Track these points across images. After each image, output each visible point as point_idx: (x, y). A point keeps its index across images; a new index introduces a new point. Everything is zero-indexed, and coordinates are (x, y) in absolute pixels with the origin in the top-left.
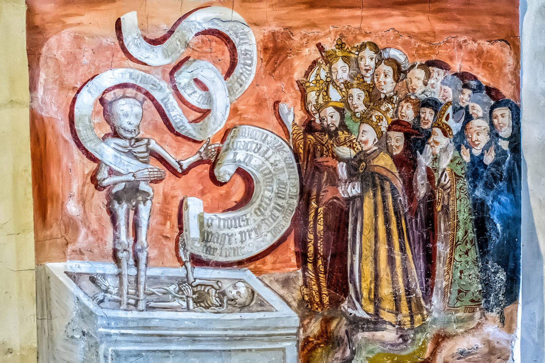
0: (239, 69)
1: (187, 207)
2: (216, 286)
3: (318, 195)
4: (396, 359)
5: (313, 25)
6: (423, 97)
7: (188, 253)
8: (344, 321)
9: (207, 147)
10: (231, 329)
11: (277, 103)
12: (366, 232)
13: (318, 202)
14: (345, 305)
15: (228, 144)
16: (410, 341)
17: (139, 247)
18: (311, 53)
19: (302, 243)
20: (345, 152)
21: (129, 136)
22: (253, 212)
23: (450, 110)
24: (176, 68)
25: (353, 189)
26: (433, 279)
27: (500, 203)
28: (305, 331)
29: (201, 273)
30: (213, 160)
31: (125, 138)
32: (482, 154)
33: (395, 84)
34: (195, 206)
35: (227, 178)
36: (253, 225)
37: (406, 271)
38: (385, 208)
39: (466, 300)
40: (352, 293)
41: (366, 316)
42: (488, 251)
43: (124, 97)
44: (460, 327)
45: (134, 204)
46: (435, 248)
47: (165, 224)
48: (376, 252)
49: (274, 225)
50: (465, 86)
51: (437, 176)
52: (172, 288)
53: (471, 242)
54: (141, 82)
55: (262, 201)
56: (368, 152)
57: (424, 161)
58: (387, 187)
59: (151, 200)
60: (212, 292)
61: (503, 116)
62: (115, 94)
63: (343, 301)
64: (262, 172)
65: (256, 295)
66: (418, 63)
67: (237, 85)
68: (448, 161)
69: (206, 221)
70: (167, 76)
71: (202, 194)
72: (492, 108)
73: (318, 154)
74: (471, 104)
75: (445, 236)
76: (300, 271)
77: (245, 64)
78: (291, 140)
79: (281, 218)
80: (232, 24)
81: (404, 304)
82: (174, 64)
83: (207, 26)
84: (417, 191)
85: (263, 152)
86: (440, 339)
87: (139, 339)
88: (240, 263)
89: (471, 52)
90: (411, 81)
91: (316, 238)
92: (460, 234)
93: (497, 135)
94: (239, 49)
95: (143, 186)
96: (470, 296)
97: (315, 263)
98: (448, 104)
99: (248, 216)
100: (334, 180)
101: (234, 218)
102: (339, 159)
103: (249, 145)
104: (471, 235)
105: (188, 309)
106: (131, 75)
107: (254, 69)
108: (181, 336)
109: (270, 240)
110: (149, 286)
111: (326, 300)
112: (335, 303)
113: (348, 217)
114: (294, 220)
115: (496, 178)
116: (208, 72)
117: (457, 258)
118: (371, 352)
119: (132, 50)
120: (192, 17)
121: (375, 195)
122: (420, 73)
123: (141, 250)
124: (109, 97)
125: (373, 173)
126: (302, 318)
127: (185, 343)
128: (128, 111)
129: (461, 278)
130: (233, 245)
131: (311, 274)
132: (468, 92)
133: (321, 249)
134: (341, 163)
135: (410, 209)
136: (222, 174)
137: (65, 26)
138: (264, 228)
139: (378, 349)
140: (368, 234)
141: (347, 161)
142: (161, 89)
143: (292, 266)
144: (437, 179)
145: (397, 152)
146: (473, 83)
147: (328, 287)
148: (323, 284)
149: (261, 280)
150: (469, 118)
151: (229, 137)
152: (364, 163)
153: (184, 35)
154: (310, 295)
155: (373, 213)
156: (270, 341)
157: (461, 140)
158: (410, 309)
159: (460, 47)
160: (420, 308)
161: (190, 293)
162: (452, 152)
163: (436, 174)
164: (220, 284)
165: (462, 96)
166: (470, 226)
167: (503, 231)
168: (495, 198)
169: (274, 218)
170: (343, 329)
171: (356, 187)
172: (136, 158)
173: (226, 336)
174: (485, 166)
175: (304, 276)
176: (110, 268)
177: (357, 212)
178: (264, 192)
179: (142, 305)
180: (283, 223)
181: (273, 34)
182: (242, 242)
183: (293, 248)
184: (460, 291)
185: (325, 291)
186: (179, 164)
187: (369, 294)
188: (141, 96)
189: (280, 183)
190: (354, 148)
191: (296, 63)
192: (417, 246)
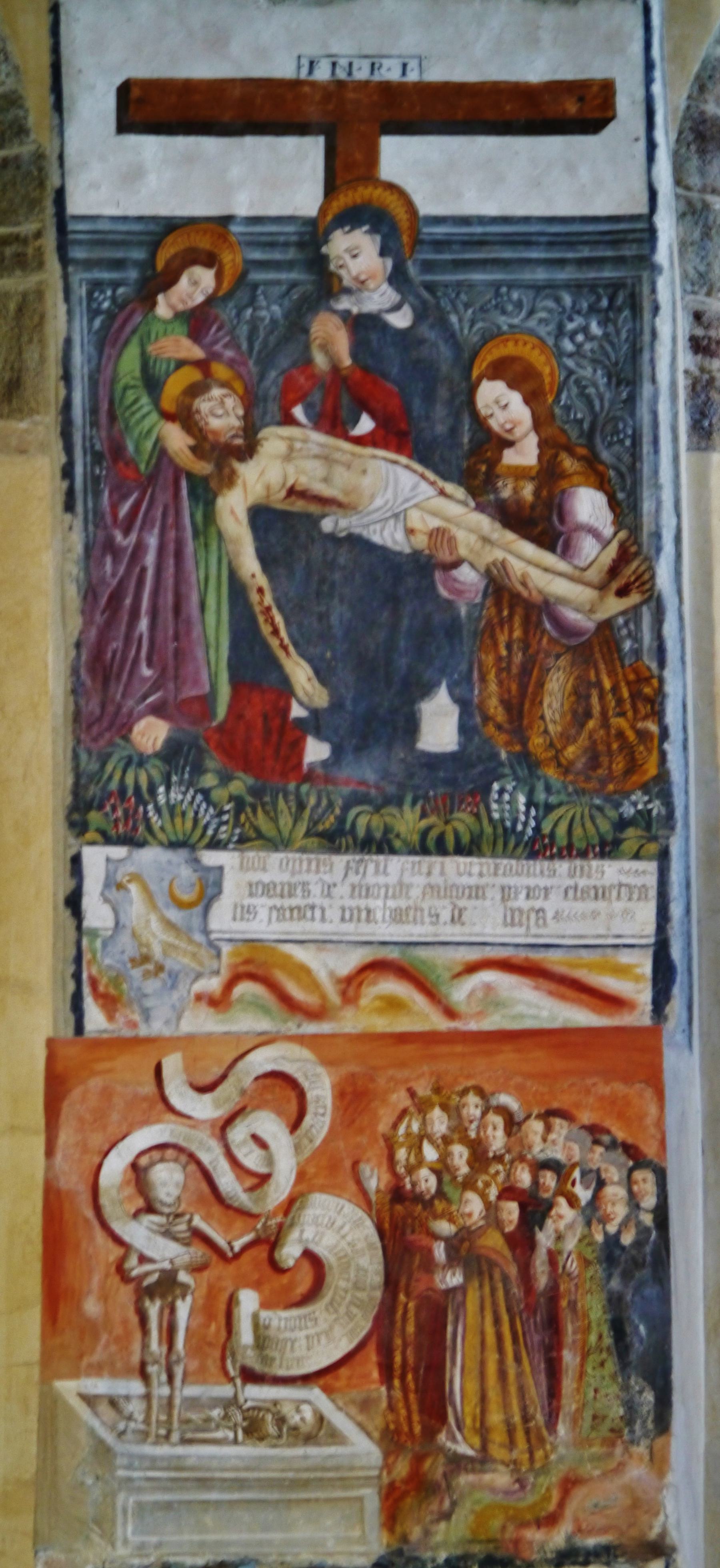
0: (308, 1120)
1: (238, 1303)
2: (273, 1409)
3: (408, 1285)
4: (511, 1512)
5: (402, 1064)
6: (542, 1157)
7: (238, 1365)
8: (441, 1460)
9: (266, 1222)
10: (290, 1470)
11: (355, 1164)
12: (469, 1337)
13: (408, 1295)
14: (442, 1437)
15: (293, 1218)
16: (529, 1488)
17: (174, 1358)
20: (444, 1227)
21: (167, 1210)
22: (323, 1307)
23: (577, 1174)
24: (229, 1121)
25: (454, 1279)
26: (559, 1401)
27: (643, 1297)
28: (389, 1473)
29: (255, 1393)
30: (273, 1238)
31: (161, 1214)
32: (619, 1232)
33: (506, 1139)
34: (248, 1301)
35: (291, 1263)
36: (323, 1326)
37: (522, 1391)
38: (495, 1304)
39: (604, 1430)
40: (451, 1419)
41: (470, 1452)
42: (630, 1363)
43: (162, 1160)
44: (595, 1468)
45: (170, 1299)
46: (560, 1359)
47: (208, 1326)
48: (483, 1364)
49: (351, 1325)
50: (596, 1142)
51: (561, 1261)
52: (216, 1413)
53: (608, 1349)
54: (184, 1140)
55: (335, 1293)
56: (473, 1228)
57: (544, 1239)
58: (497, 1276)
59: (192, 1293)
60: (269, 1417)
61: (644, 1180)
62: (151, 1157)
63: (439, 1431)
64: (336, 1254)
65: (325, 1423)
66: (535, 1112)
67: (305, 1141)
68: (576, 1240)
69: (261, 1322)
70: (217, 1131)
71: (257, 1285)
72: (631, 1171)
73: (409, 1231)
74: (603, 1166)
75: (574, 1342)
76: (383, 1389)
77: (316, 1114)
78: (374, 1212)
79: (360, 1315)
80: (298, 1064)
81: (520, 1436)
82: (226, 1116)
83: (269, 1067)
84: (536, 1280)
85: (338, 1229)
86: (569, 1484)
87: (169, 1484)
88: (306, 1379)
89: (602, 1098)
90: (527, 1137)
91: (405, 1345)
92: (593, 1338)
93: (637, 1207)
94: (310, 1095)
95: (183, 1277)
96: (608, 1424)
97: (403, 1378)
98: (574, 1166)
99: (317, 1314)
100: (429, 1265)
101: (300, 1318)
102: (436, 1237)
103: (320, 1220)
104: (608, 1341)
105: (235, 1442)
106: (172, 1132)
107: (327, 1119)
108: (224, 1480)
109: (344, 1347)
110: (187, 1410)
111: (417, 1429)
112: (430, 1434)
113: (446, 1316)
114: (377, 1320)
115: (638, 1264)
116: (268, 1124)
117: (589, 1370)
118: (478, 1502)
119: (175, 1101)
120: (251, 1057)
121: (481, 1286)
122: (537, 1126)
123: (178, 1361)
124: (144, 1161)
125: (479, 1258)
126: (386, 1455)
127: (230, 1489)
128: (167, 1179)
129: (595, 1398)
130: (297, 1353)
131: (398, 1394)
132: (600, 1150)
133: (411, 1360)
134: (438, 1243)
135: (527, 1305)
136: (284, 1257)
137: (93, 1073)
138: (338, 1331)
139: (487, 1498)
140: (473, 1340)
141: (447, 1240)
142: (209, 1150)
143: (373, 1382)
144: (561, 1264)
145: (509, 1229)
146: (606, 1139)
147: (421, 1411)
148: (415, 1407)
149: (333, 1401)
150: (601, 1184)
151: (294, 1208)
152: (466, 1245)
153: (239, 1080)
154: (397, 1422)
155: (477, 1309)
156: (345, 1488)
157: (593, 1212)
158: (528, 1441)
159: (588, 1092)
160: (542, 1441)
161: (239, 1418)
162: (579, 1230)
163: (560, 1258)
164: (278, 1407)
165: (590, 1156)
166: (605, 1329)
167: (649, 1334)
168: (637, 1290)
169: (350, 1316)
170: (440, 1470)
171: (457, 1274)
172: (176, 1239)
173: (284, 1479)
174: (623, 1248)
175: (390, 1397)
177: (458, 1308)
178: (336, 1282)
179: (175, 1437)
180: (363, 1323)
181: (353, 1075)
182: (309, 1349)
183: (374, 1358)
184: (595, 1417)
185: (416, 1417)
186: (229, 1243)
187: (474, 1420)
188: (183, 1158)
189: (359, 1269)
190: (454, 1223)
191: (382, 1112)
192: (537, 1356)
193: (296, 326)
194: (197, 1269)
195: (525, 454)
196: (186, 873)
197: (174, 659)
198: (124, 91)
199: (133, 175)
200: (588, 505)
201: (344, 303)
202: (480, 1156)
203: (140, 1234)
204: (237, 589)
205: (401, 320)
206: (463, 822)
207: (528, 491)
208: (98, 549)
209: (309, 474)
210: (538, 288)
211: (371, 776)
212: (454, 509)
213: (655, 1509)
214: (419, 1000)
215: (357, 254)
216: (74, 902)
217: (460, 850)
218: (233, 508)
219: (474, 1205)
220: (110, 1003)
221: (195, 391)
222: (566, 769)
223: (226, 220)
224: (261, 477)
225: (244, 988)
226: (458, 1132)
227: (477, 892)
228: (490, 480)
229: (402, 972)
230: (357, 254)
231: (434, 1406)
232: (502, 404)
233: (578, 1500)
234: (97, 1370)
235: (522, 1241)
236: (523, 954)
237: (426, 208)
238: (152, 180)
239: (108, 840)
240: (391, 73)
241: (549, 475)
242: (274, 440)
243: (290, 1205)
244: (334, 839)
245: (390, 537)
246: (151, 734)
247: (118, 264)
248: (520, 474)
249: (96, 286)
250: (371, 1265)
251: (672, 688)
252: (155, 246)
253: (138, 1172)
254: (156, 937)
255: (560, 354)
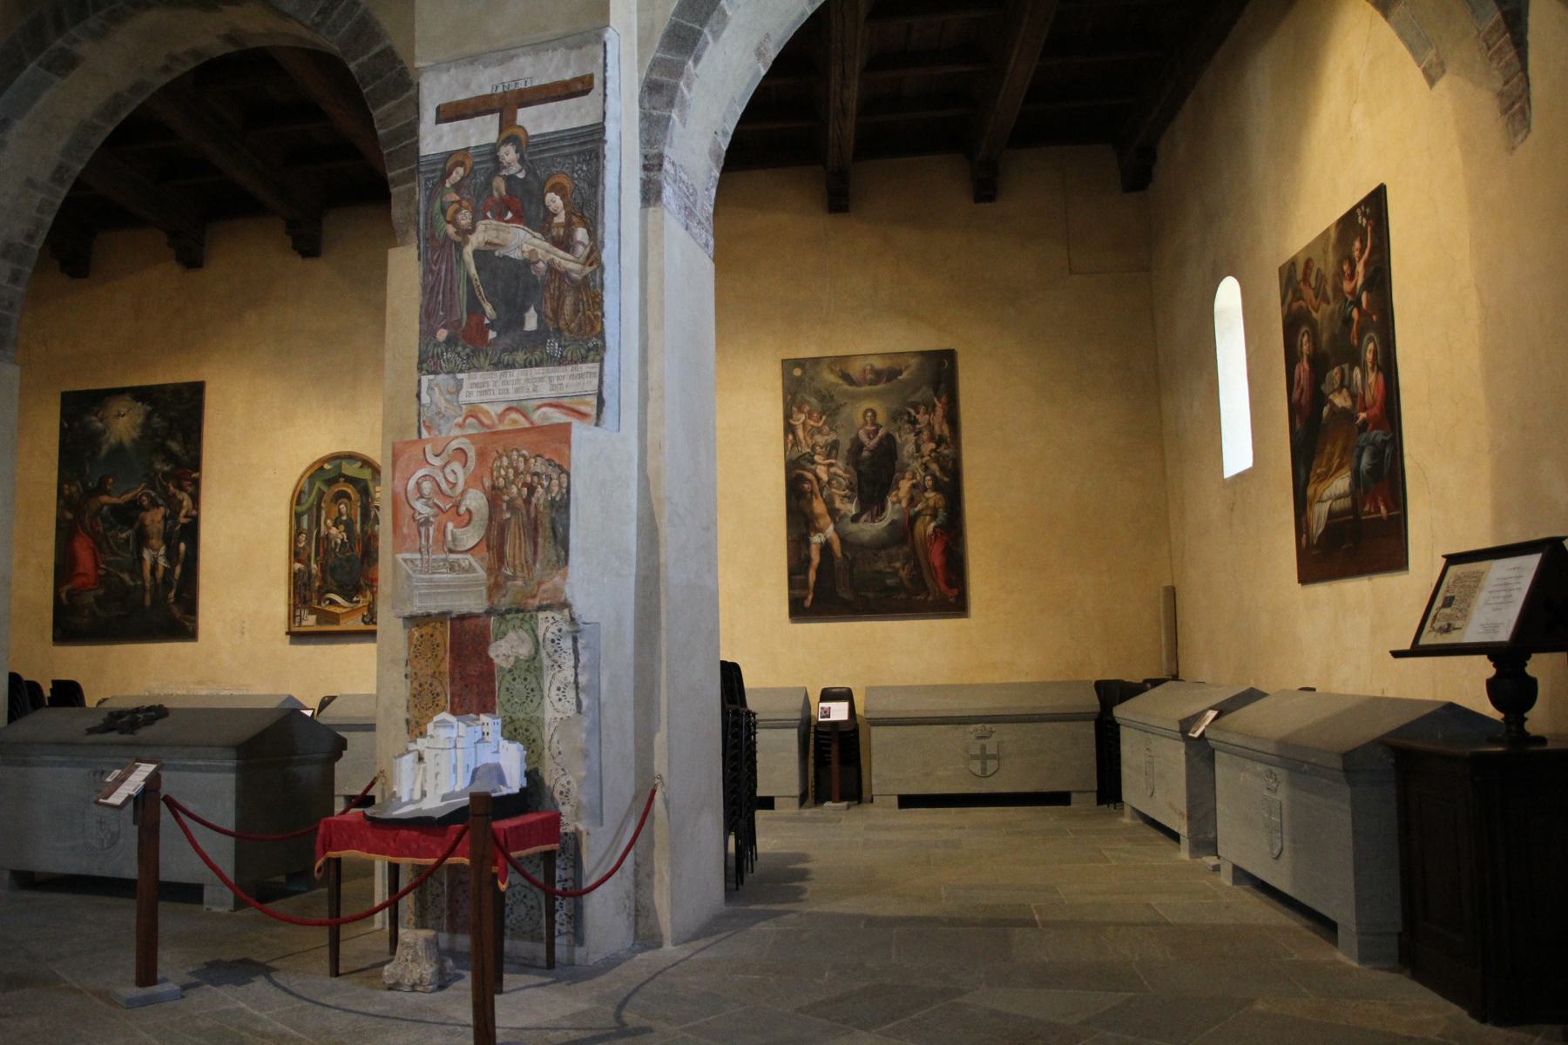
18: (494, 454)
19: (488, 540)
20: (506, 498)
34: (450, 526)
57: (534, 500)
85: (476, 501)
86: (540, 584)
88: (467, 551)
116: (456, 466)
128: (427, 486)
157: (548, 490)
176: (418, 556)
178: (475, 518)
193: (488, 184)
194: (435, 516)
195: (561, 218)
196: (452, 382)
197: (450, 308)
198: (438, 109)
199: (440, 138)
200: (581, 234)
201: (504, 173)
202: (517, 473)
203: (419, 505)
204: (469, 280)
205: (521, 176)
206: (537, 355)
207: (561, 232)
208: (428, 271)
209: (491, 236)
210: (566, 156)
211: (508, 341)
212: (537, 242)
213: (562, 591)
214: (522, 419)
215: (509, 154)
216: (418, 396)
217: (537, 365)
218: (468, 251)
219: (514, 490)
220: (429, 429)
221: (457, 212)
222: (571, 332)
223: (467, 149)
224: (476, 240)
225: (470, 420)
226: (510, 465)
227: (541, 380)
228: (549, 230)
229: (517, 410)
230: (509, 154)
231: (501, 558)
232: (554, 201)
233: (543, 587)
234: (407, 551)
235: (527, 501)
236: (554, 401)
237: (531, 132)
238: (445, 140)
239: (429, 373)
240: (522, 85)
241: (569, 225)
242: (481, 226)
243: (463, 493)
244: (498, 365)
245: (516, 255)
246: (442, 334)
247: (434, 171)
248: (559, 225)
249: (428, 179)
250: (485, 511)
251: (606, 299)
252: (446, 160)
253: (418, 484)
254: (443, 404)
255: (573, 179)
